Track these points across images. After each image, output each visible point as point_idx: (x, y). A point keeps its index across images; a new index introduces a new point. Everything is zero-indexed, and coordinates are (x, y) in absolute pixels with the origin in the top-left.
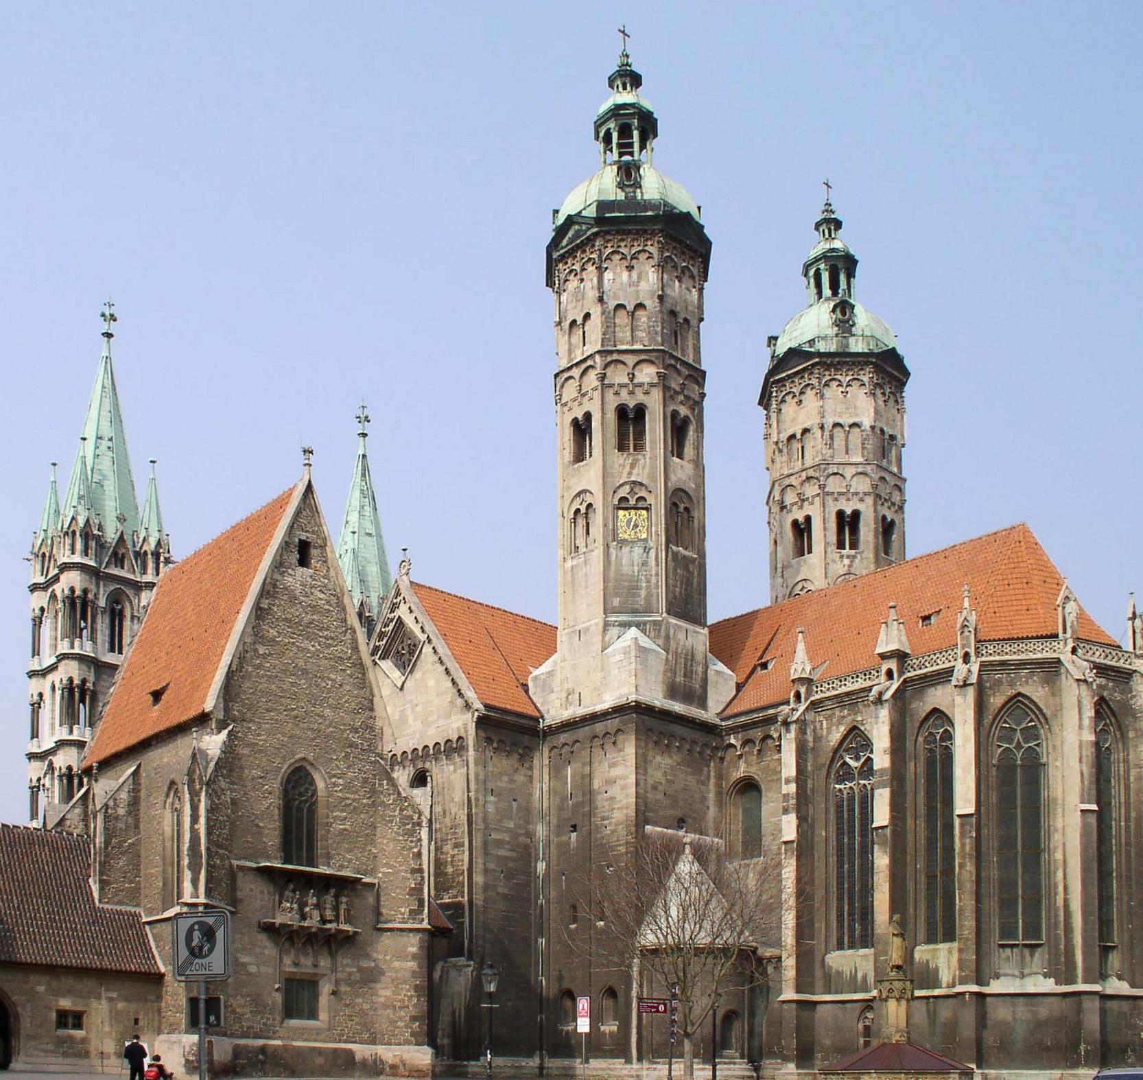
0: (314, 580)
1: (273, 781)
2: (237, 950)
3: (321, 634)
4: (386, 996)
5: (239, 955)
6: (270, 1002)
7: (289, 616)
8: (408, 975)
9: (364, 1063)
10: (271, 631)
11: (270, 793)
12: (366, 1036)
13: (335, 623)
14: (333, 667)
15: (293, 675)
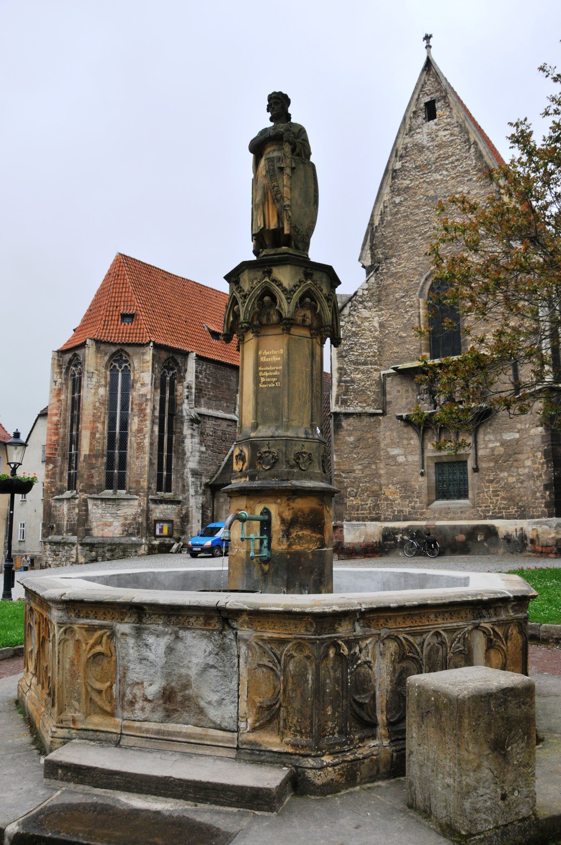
0: (439, 125)
1: (413, 296)
2: (387, 445)
3: (447, 162)
4: (528, 467)
5: (389, 449)
6: (417, 487)
7: (418, 164)
8: (539, 440)
9: (508, 539)
10: (404, 182)
11: (411, 306)
12: (513, 510)
13: (459, 147)
14: (458, 182)
15: (425, 206)
